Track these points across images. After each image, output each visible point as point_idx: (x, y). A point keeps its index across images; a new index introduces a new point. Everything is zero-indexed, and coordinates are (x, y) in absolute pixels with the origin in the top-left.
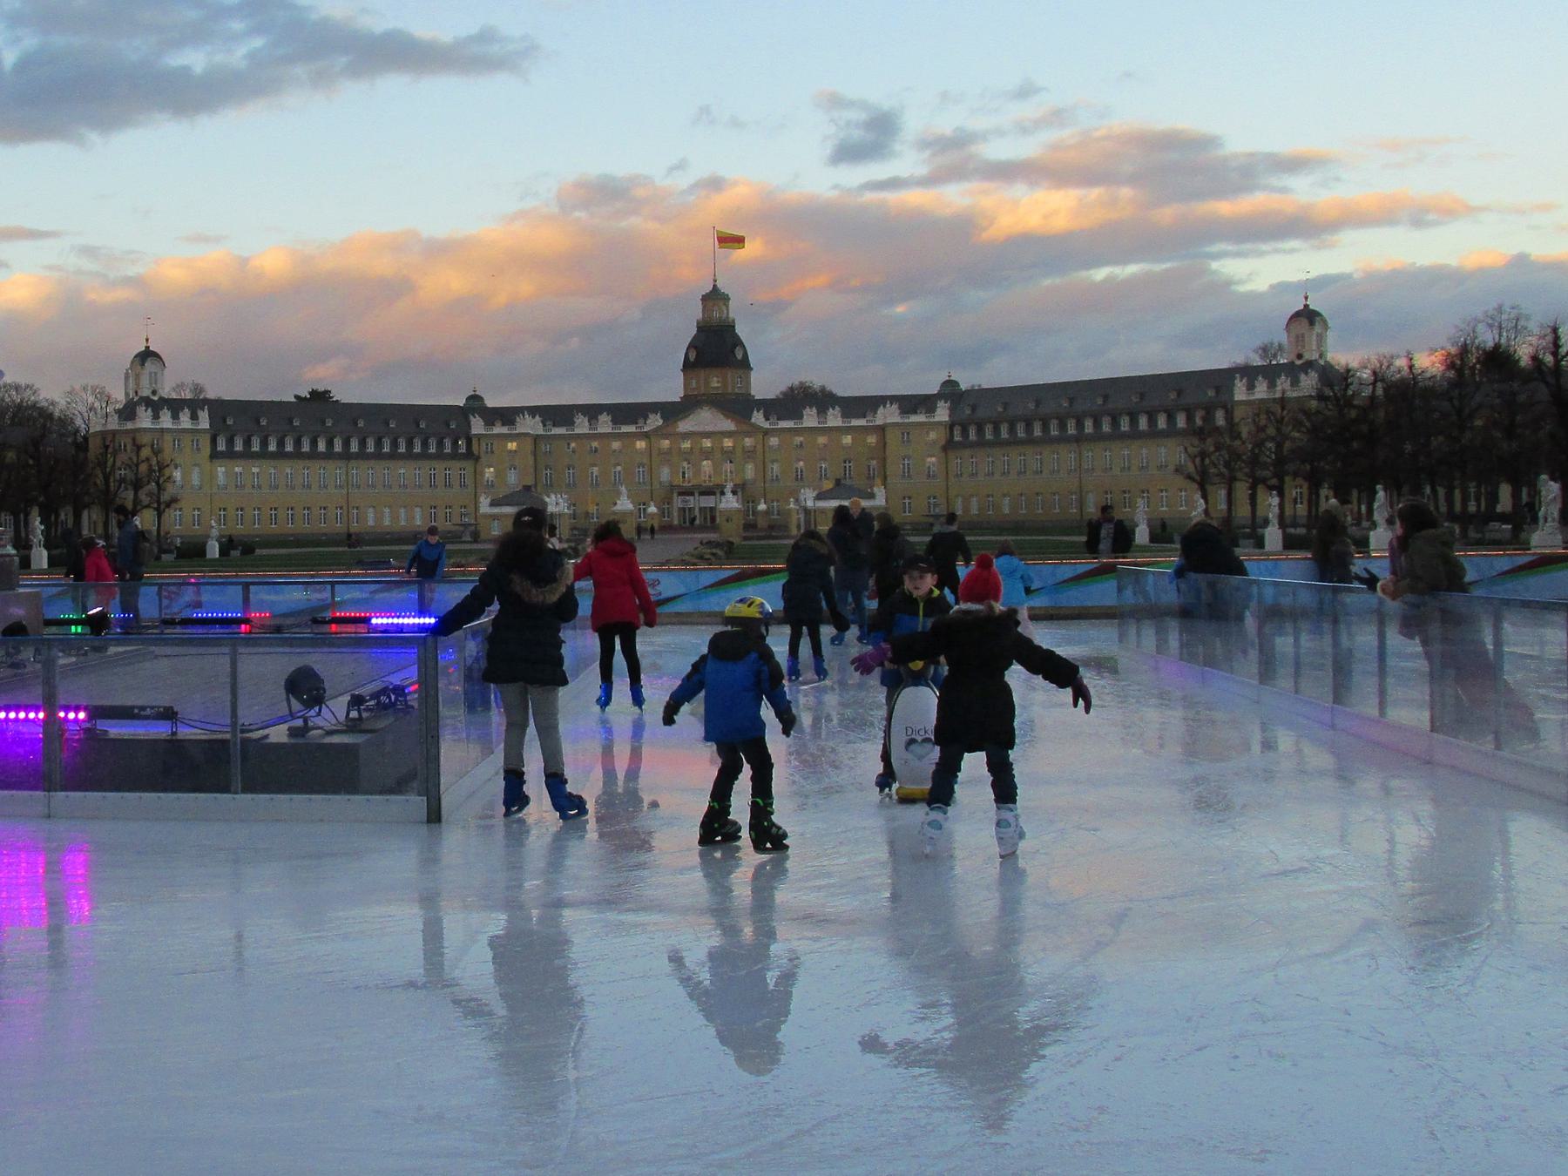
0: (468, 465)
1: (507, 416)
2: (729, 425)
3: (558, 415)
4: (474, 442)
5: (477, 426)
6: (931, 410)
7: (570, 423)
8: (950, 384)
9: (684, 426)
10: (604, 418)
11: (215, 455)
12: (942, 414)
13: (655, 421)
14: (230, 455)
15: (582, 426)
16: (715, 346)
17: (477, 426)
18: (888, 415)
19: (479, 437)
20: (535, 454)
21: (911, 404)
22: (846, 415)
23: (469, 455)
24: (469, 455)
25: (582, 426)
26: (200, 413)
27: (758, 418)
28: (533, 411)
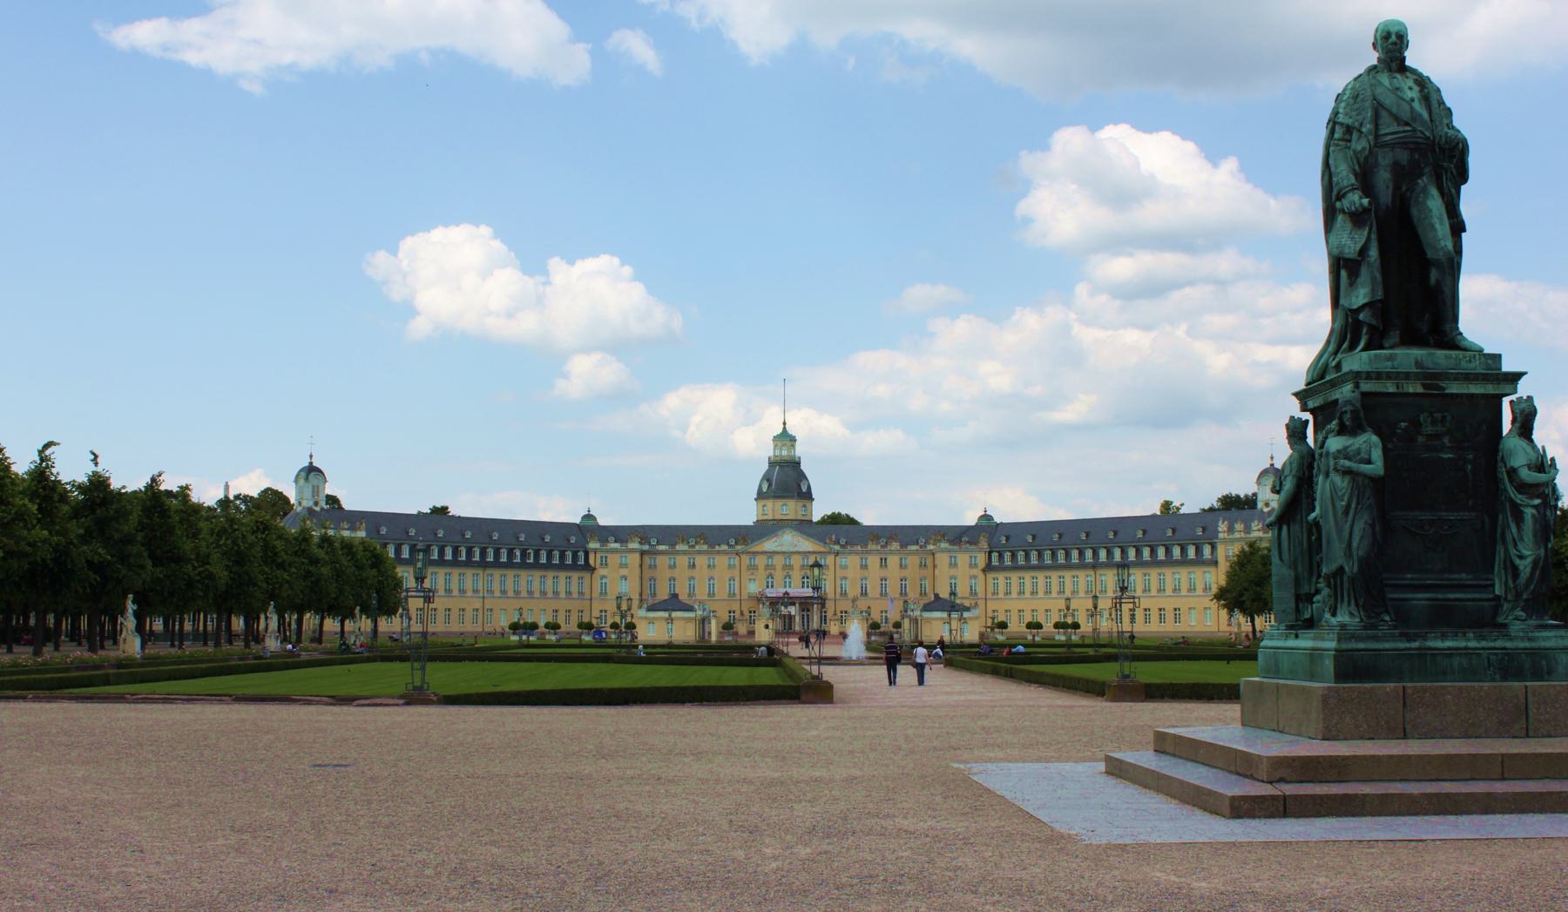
0: (587, 575)
1: (621, 534)
2: (806, 545)
4: (591, 556)
9: (769, 545)
16: (786, 479)
23: (588, 568)
24: (588, 568)
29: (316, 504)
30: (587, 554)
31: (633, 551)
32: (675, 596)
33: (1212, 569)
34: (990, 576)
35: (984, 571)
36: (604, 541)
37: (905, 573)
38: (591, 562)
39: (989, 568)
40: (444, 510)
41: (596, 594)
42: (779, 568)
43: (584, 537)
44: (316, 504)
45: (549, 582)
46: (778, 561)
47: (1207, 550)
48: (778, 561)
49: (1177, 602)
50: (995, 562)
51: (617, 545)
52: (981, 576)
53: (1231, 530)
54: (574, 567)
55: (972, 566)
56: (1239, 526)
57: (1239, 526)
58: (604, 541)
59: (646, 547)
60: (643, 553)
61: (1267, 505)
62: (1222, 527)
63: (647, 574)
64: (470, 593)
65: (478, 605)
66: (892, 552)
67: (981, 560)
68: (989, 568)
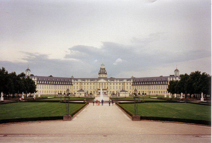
1: (77, 79)
3: (84, 79)
5: (73, 81)
6: (130, 81)
7: (85, 81)
8: (132, 77)
9: (99, 81)
10: (89, 80)
12: (132, 81)
13: (96, 81)
15: (86, 81)
16: (103, 71)
18: (125, 81)
20: (80, 84)
21: (128, 80)
22: (120, 81)
23: (72, 85)
24: (72, 85)
25: (86, 81)
27: (109, 81)
28: (80, 79)
30: (72, 82)
31: (79, 82)
32: (82, 89)
36: (74, 80)
38: (72, 84)
40: (51, 76)
43: (71, 80)
44: (29, 75)
45: (51, 86)
46: (101, 84)
48: (101, 84)
49: (146, 90)
51: (76, 81)
52: (131, 85)
53: (170, 79)
54: (70, 85)
55: (130, 84)
58: (74, 80)
59: (81, 82)
60: (80, 82)
62: (169, 78)
63: (81, 85)
64: (53, 88)
65: (54, 90)
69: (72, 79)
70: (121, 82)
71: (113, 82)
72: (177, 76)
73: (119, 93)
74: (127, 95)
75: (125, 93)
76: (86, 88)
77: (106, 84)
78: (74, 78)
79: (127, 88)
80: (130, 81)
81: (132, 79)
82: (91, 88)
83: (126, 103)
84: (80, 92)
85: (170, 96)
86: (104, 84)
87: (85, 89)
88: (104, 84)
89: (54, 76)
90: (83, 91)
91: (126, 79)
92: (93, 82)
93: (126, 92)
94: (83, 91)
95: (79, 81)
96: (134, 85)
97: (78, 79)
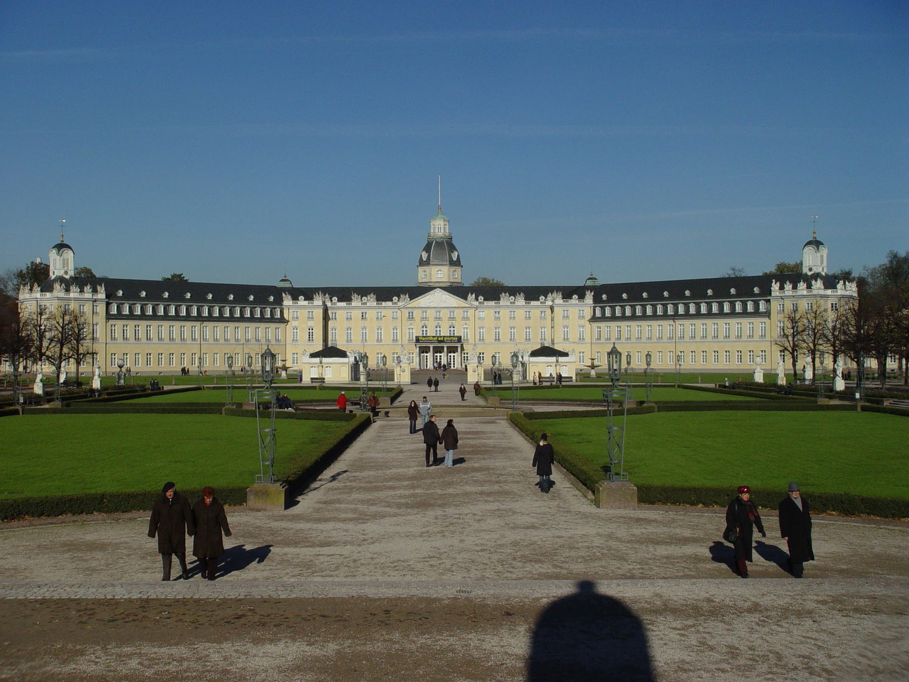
0: (282, 326)
2: (453, 301)
5: (287, 301)
6: (582, 297)
9: (423, 301)
11: (109, 317)
12: (589, 298)
14: (119, 316)
17: (287, 301)
19: (289, 308)
23: (282, 320)
24: (282, 320)
26: (99, 288)
29: (66, 273)
33: (766, 320)
34: (595, 325)
35: (589, 321)
36: (295, 298)
37: (530, 323)
38: (286, 316)
39: (594, 319)
41: (289, 340)
42: (431, 319)
44: (66, 273)
47: (762, 307)
48: (431, 314)
50: (598, 314)
51: (306, 303)
53: (782, 288)
54: (272, 320)
56: (788, 286)
57: (788, 286)
58: (295, 298)
61: (810, 270)
62: (775, 286)
64: (189, 341)
66: (519, 307)
67: (588, 313)
68: (594, 319)
69: (284, 290)
70: (533, 303)
71: (492, 303)
72: (816, 276)
73: (523, 364)
74: (568, 369)
75: (554, 359)
76: (356, 337)
77: (458, 314)
78: (296, 285)
79: (566, 339)
80: (582, 297)
81: (591, 288)
82: (379, 340)
83: (574, 414)
84: (325, 360)
85: (782, 369)
86: (445, 314)
87: (349, 341)
88: (445, 314)
89: (192, 277)
90: (343, 354)
91: (557, 289)
92: (389, 304)
93: (561, 359)
94: (343, 354)
95: (318, 301)
96: (603, 318)
97: (316, 290)
